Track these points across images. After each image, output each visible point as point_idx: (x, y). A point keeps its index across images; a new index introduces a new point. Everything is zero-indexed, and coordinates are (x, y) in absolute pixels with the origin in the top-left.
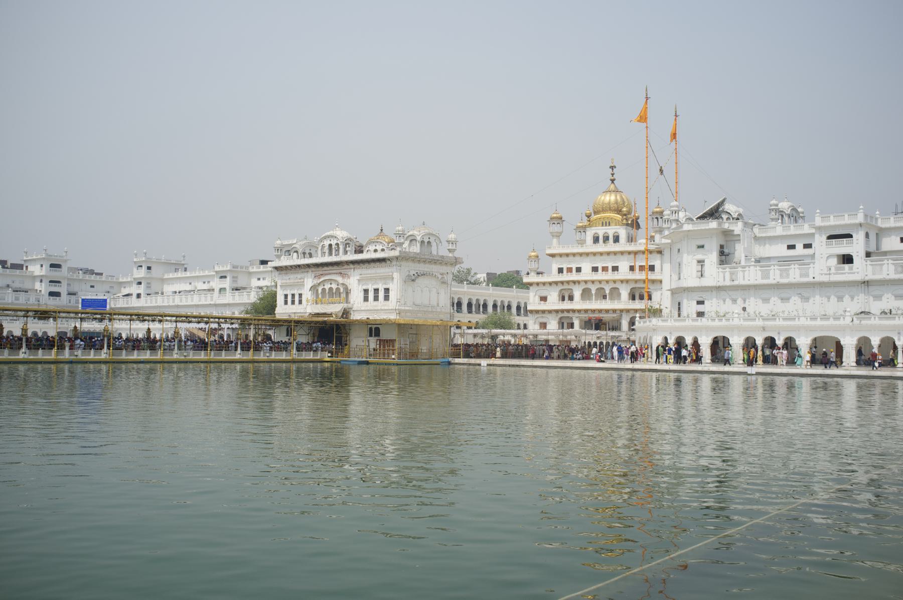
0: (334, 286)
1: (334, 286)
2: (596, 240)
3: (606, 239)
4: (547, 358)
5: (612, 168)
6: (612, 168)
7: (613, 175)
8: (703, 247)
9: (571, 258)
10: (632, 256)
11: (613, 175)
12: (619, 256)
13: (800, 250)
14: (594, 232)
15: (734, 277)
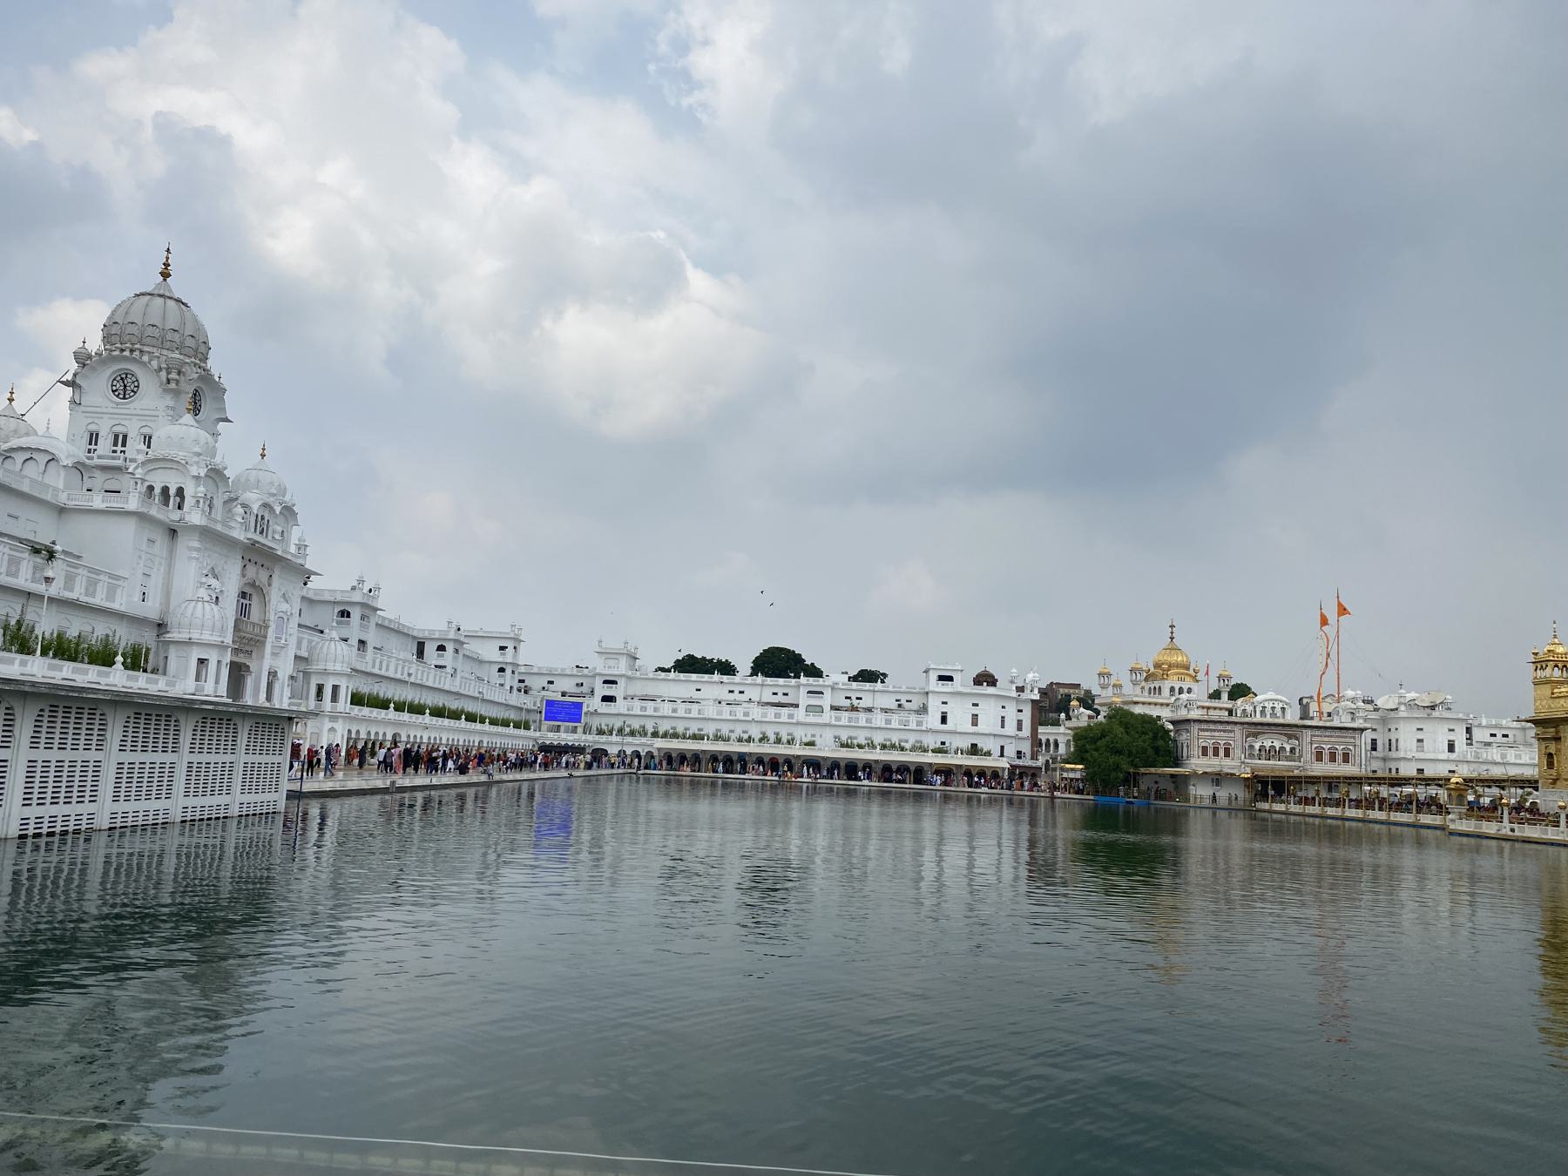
0: (1277, 745)
1: (1277, 745)
2: (1172, 689)
3: (1181, 691)
4: (660, 770)
5: (1172, 626)
6: (1172, 626)
7: (1172, 633)
8: (1453, 730)
9: (1152, 706)
10: (1205, 710)
11: (1172, 633)
12: (1158, 707)
13: (1499, 738)
14: (1171, 685)
15: (1480, 755)
